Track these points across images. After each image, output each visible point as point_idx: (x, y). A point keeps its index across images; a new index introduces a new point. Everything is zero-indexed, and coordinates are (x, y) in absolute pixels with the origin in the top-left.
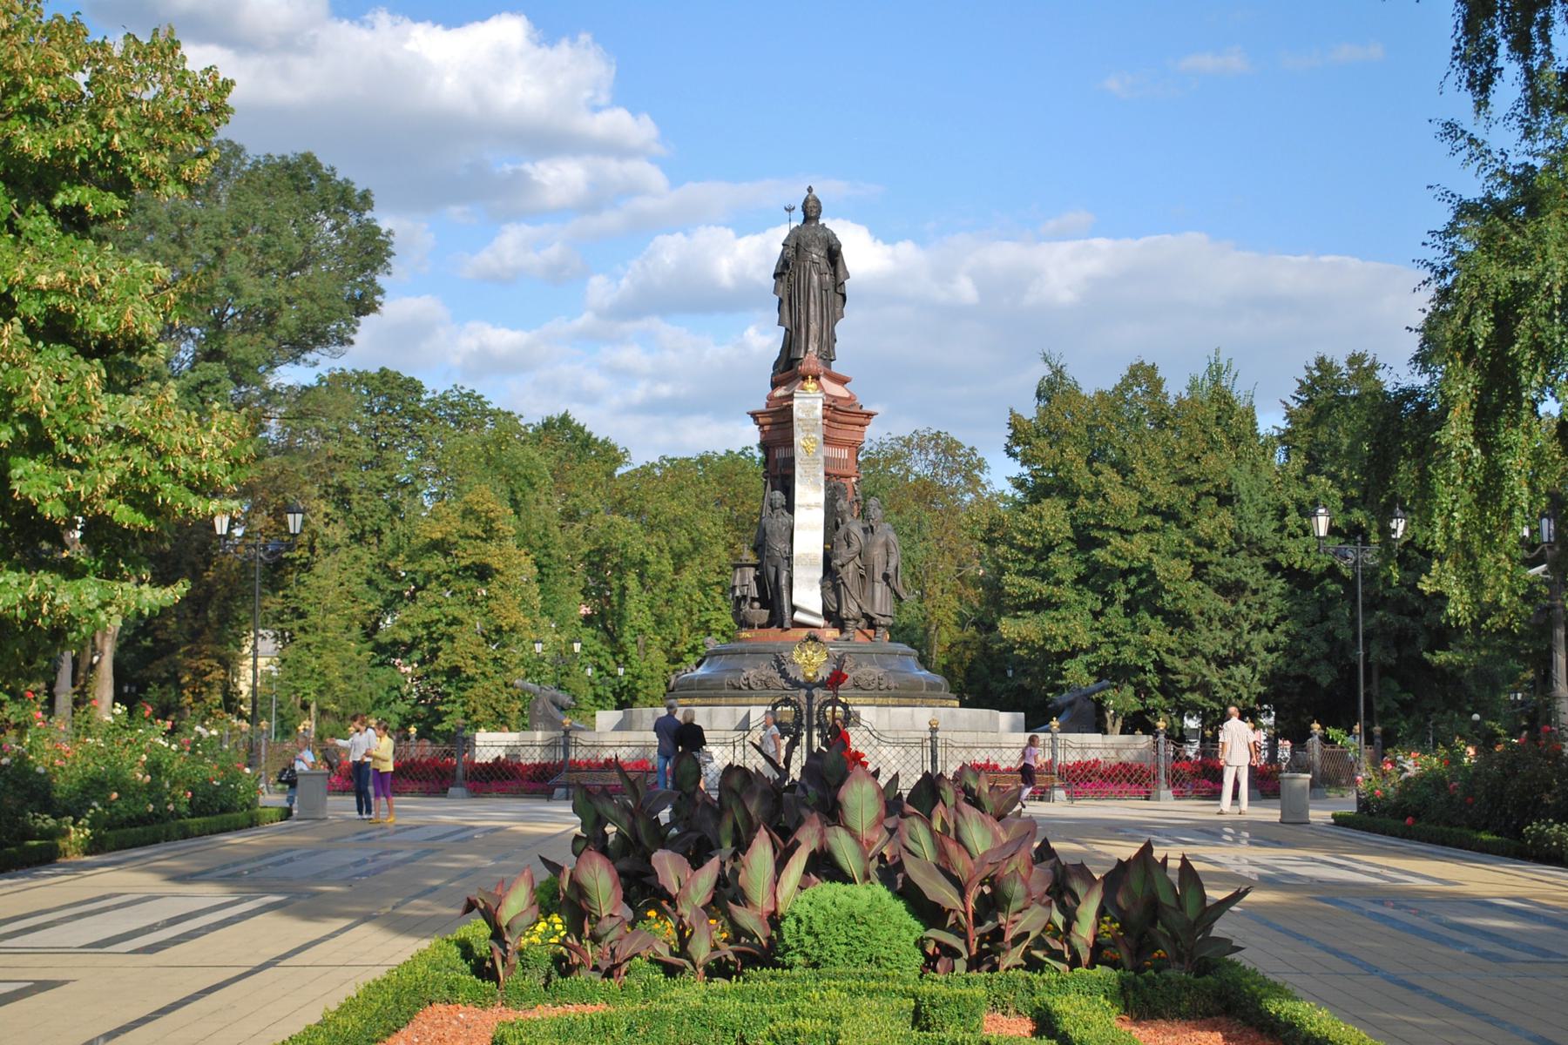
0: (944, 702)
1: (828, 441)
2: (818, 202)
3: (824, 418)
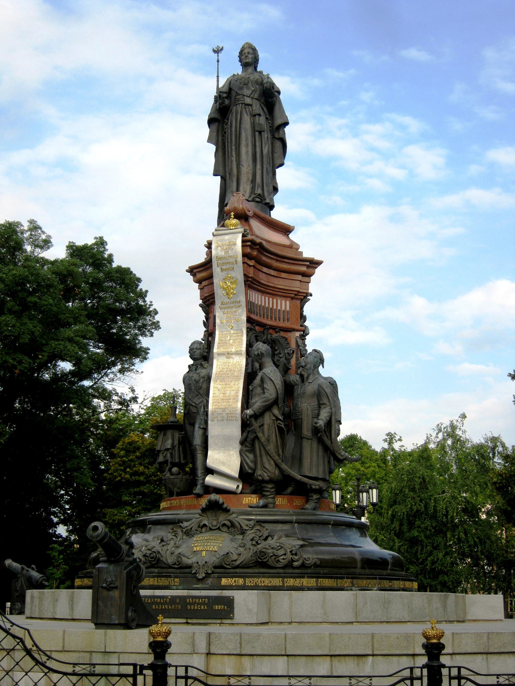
0: (386, 584)
2: (254, 50)
3: (244, 255)
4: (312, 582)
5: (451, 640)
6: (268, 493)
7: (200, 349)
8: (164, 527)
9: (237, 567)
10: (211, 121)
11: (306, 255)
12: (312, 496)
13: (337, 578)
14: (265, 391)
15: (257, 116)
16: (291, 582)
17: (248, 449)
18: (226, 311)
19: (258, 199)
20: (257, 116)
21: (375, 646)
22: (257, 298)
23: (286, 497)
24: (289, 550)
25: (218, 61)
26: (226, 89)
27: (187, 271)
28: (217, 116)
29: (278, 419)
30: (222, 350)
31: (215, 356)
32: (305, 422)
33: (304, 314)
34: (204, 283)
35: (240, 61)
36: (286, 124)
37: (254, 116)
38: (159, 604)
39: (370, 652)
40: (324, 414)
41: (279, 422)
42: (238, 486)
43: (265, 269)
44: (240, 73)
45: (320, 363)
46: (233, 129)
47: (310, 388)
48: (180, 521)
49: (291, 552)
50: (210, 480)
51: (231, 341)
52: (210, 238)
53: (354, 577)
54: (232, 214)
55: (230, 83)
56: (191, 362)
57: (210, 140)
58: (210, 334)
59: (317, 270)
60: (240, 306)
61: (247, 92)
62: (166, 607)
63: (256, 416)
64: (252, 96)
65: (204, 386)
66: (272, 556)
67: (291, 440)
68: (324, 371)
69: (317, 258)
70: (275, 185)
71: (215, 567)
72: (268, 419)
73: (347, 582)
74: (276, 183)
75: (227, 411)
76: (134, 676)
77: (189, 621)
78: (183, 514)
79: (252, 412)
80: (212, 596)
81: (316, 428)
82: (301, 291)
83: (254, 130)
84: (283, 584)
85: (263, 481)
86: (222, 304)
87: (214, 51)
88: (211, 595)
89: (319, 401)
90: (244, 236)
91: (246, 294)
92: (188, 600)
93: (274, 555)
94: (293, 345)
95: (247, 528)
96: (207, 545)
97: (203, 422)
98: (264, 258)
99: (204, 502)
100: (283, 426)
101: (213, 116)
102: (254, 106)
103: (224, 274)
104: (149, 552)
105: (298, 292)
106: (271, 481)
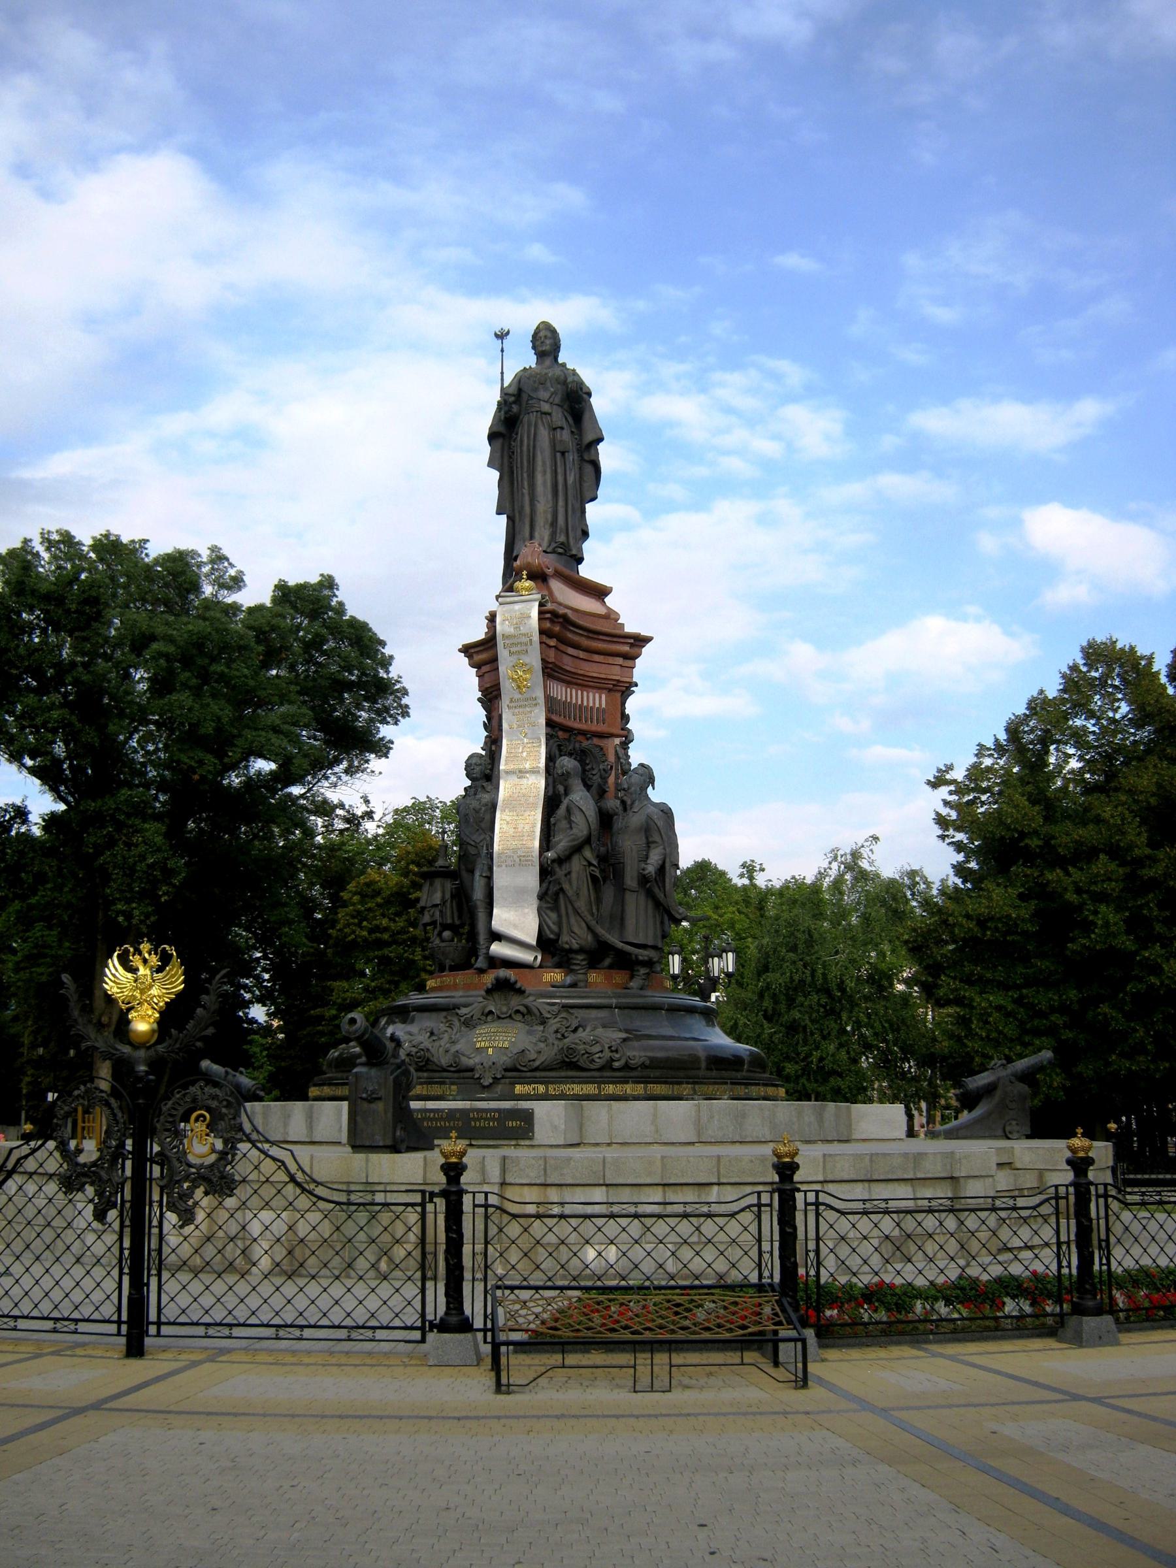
0: (741, 1090)
1: (550, 671)
3: (542, 632)
4: (640, 1089)
5: (821, 1164)
6: (577, 968)
7: (480, 765)
8: (434, 1015)
9: (536, 1069)
10: (492, 437)
11: (629, 629)
12: (638, 971)
13: (672, 1083)
14: (573, 825)
15: (558, 430)
16: (610, 1089)
17: (549, 905)
18: (516, 711)
19: (560, 550)
20: (558, 430)
21: (722, 1171)
22: (560, 691)
23: (603, 972)
24: (607, 1046)
25: (502, 351)
26: (513, 390)
27: (460, 650)
28: (502, 429)
29: (590, 864)
30: (511, 767)
31: (502, 774)
32: (629, 868)
33: (627, 712)
34: (485, 669)
35: (534, 348)
36: (601, 439)
37: (555, 429)
38: (431, 1120)
39: (715, 1180)
40: (655, 857)
41: (592, 868)
42: (536, 958)
43: (571, 651)
44: (534, 366)
45: (649, 782)
46: (525, 448)
47: (635, 820)
48: (456, 1007)
49: (610, 1048)
50: (497, 948)
51: (525, 754)
52: (494, 606)
53: (696, 1081)
54: (525, 573)
55: (519, 381)
56: (468, 783)
57: (491, 464)
58: (493, 742)
59: (644, 650)
60: (536, 705)
61: (544, 395)
62: (442, 1123)
63: (560, 861)
64: (551, 400)
65: (487, 817)
66: (583, 1054)
67: (609, 893)
68: (655, 795)
69: (644, 633)
70: (584, 528)
71: (506, 1070)
72: (576, 864)
73: (686, 1089)
74: (587, 526)
75: (520, 853)
76: (423, 1205)
77: (474, 1142)
78: (461, 997)
79: (555, 856)
80: (504, 1109)
81: (644, 876)
82: (622, 679)
83: (554, 450)
84: (600, 1091)
85: (571, 951)
86: (511, 701)
87: (497, 336)
88: (503, 1107)
89: (647, 838)
90: (541, 605)
91: (545, 687)
92: (471, 1115)
93: (587, 1053)
94: (612, 758)
95: (549, 1016)
96: (494, 1040)
97: (486, 868)
98: (570, 635)
99: (489, 979)
100: (598, 874)
101: (495, 429)
102: (554, 414)
103: (513, 659)
104: (414, 1050)
105: (618, 681)
106: (581, 950)
